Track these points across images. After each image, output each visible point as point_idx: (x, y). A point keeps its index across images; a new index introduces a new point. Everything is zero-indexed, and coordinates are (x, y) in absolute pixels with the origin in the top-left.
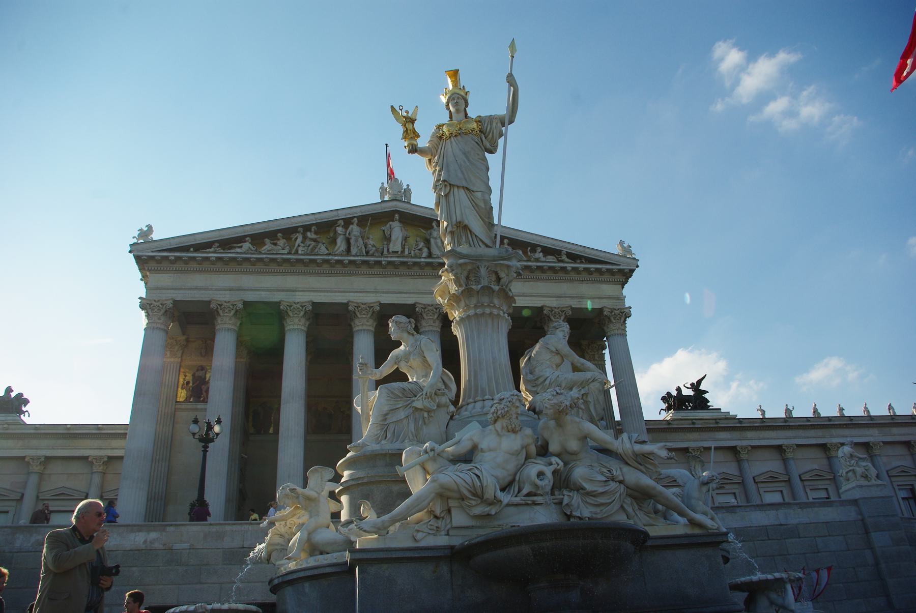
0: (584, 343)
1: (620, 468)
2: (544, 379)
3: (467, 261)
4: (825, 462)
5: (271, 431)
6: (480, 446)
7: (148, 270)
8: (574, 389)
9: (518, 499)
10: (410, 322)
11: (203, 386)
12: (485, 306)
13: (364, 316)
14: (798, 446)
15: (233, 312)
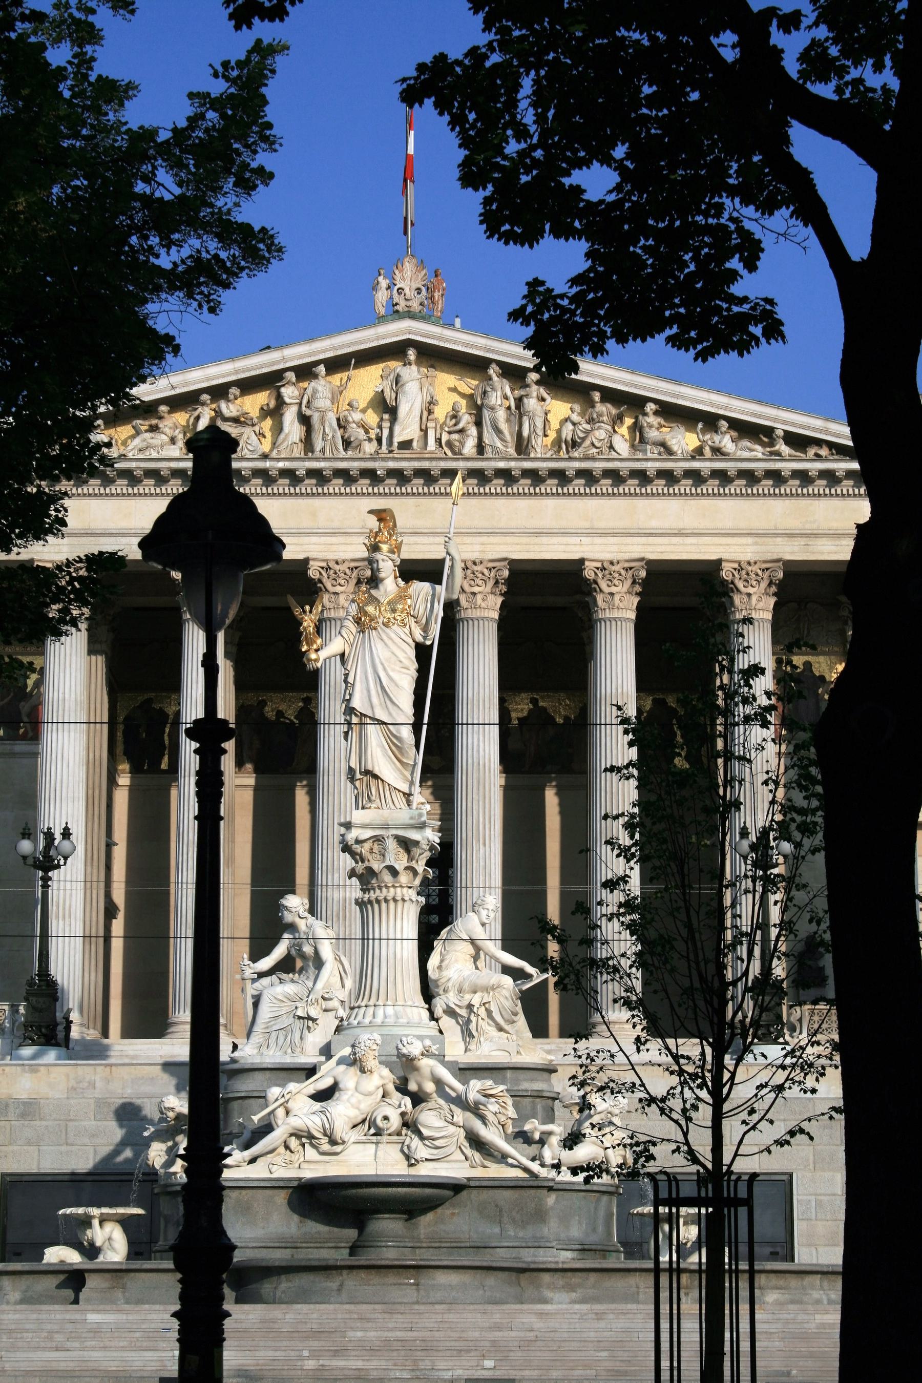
5: (164, 765)
11: (22, 703)
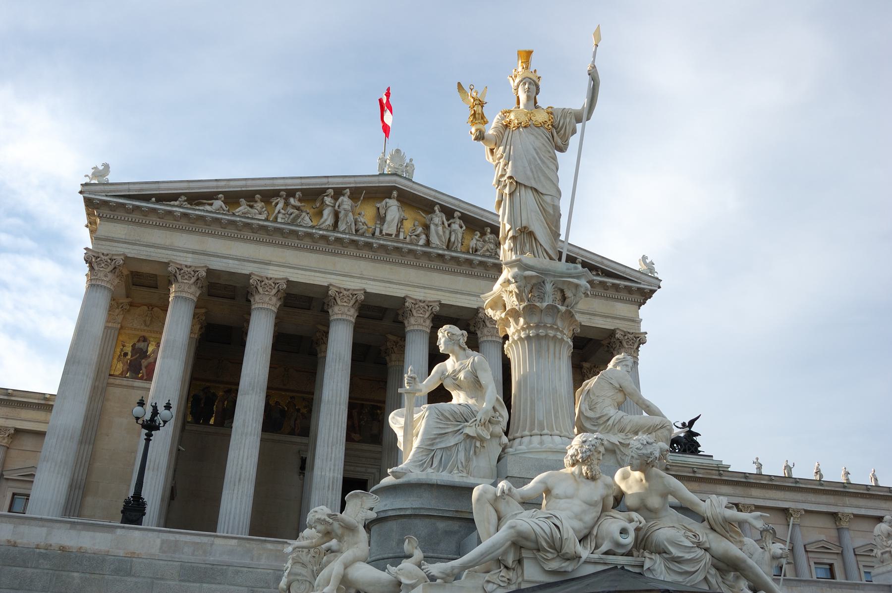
0: (586, 365)
1: (706, 534)
2: (607, 418)
3: (534, 273)
4: (834, 533)
5: (212, 422)
6: (555, 491)
7: (99, 216)
8: (640, 433)
9: (595, 556)
10: (462, 334)
11: (143, 360)
12: (548, 327)
13: (345, 304)
14: (806, 511)
15: (193, 280)
